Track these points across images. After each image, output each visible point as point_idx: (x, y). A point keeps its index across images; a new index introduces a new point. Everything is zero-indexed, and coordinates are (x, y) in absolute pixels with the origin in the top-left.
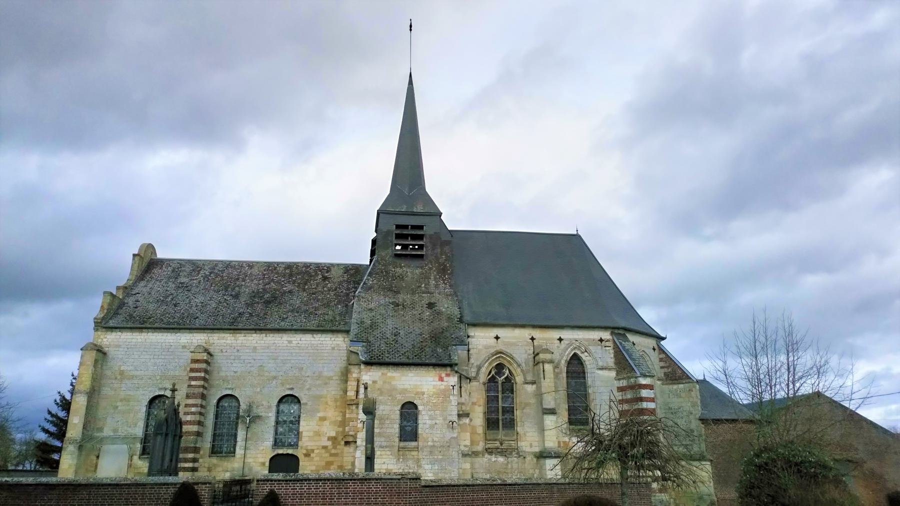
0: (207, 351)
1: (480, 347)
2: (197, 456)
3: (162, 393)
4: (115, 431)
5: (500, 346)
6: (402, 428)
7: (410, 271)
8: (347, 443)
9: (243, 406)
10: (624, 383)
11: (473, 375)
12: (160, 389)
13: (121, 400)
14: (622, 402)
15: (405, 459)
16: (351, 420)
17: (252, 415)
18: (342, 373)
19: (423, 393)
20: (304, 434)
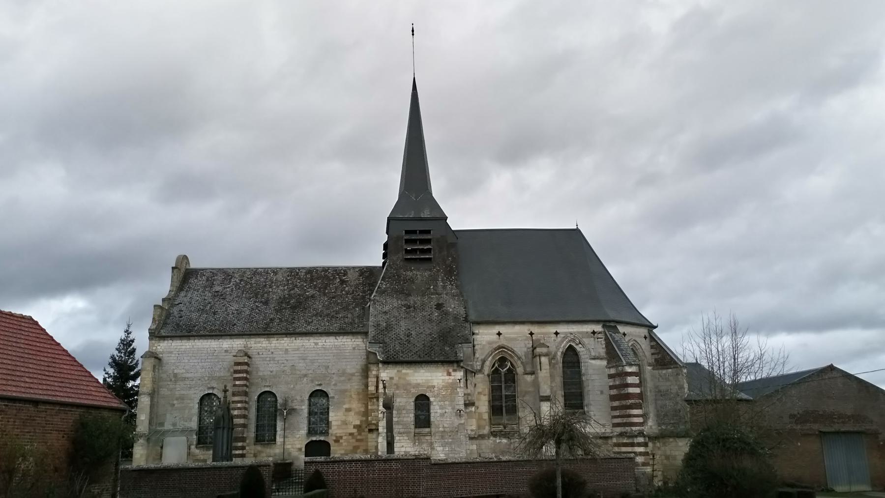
0: (246, 355)
1: (484, 343)
2: (245, 444)
3: (211, 392)
4: (174, 425)
5: (502, 341)
7: (420, 274)
8: (371, 431)
9: (280, 401)
10: (613, 371)
11: (479, 368)
12: (209, 388)
13: (177, 399)
14: (611, 388)
15: (420, 443)
16: (373, 411)
17: (288, 408)
18: (363, 369)
19: (434, 387)
20: (334, 423)
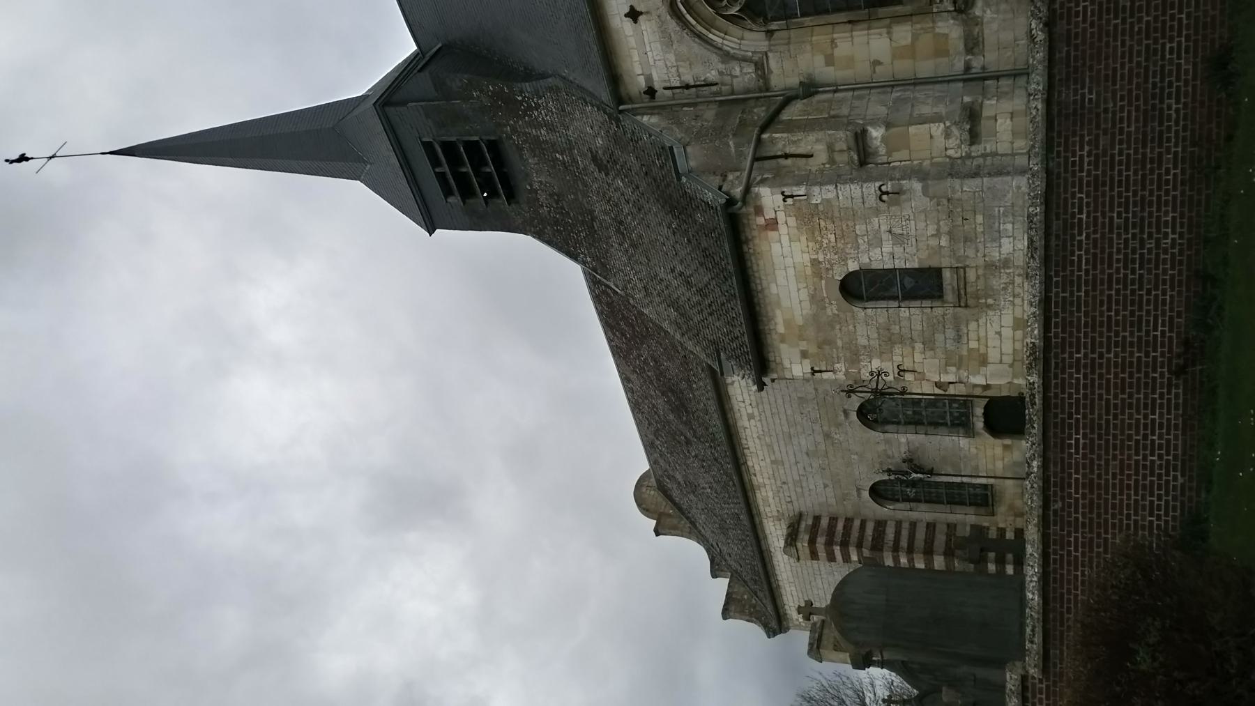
1: (671, 57)
6: (910, 295)
11: (750, 69)
19: (815, 263)
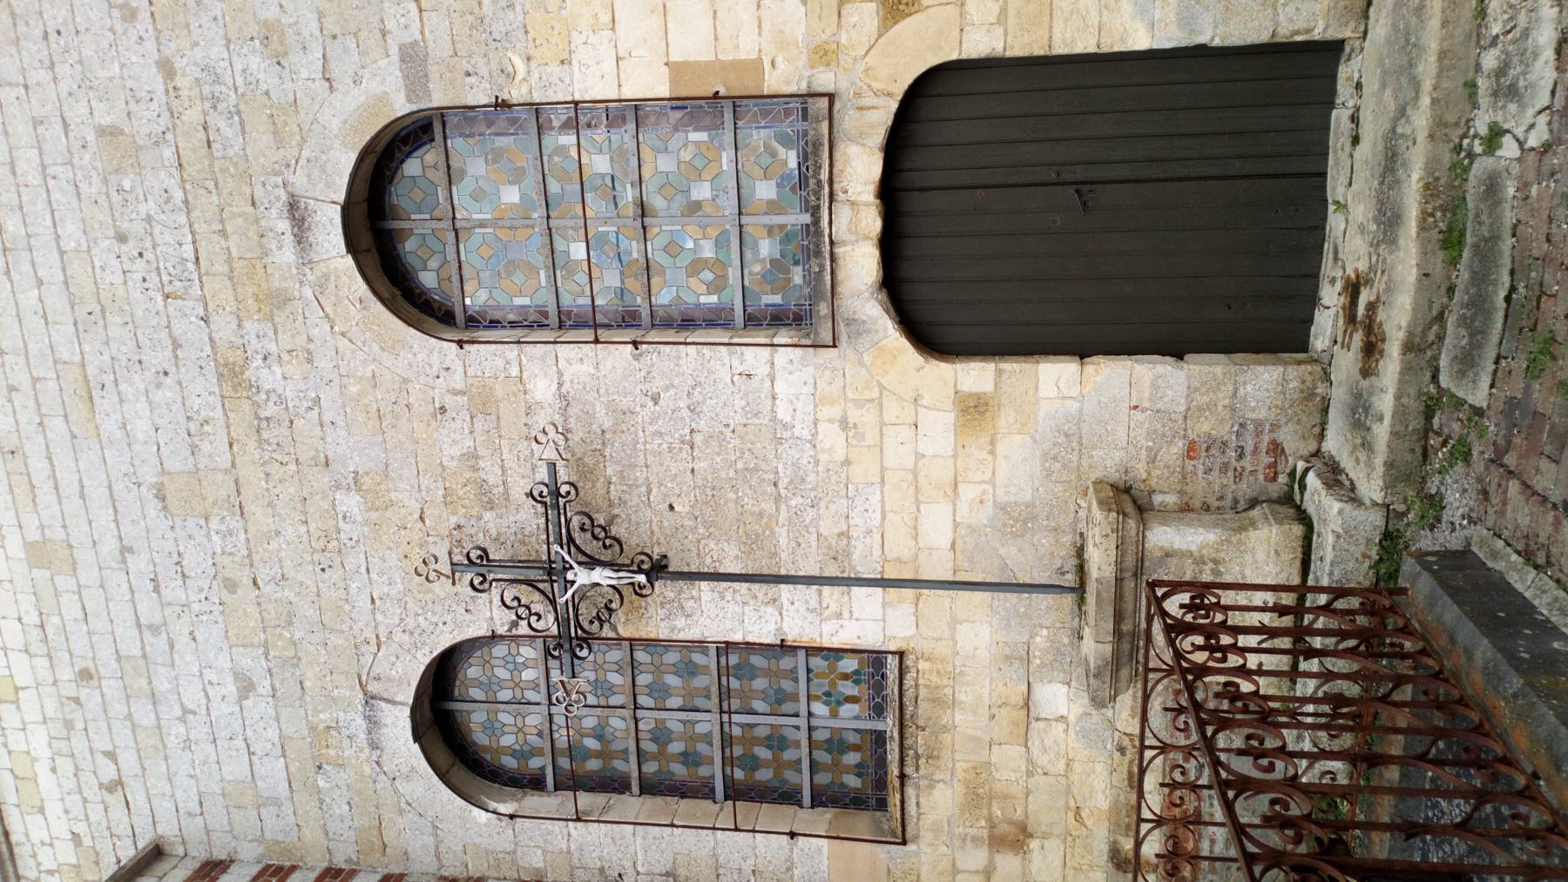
9: (486, 614)
